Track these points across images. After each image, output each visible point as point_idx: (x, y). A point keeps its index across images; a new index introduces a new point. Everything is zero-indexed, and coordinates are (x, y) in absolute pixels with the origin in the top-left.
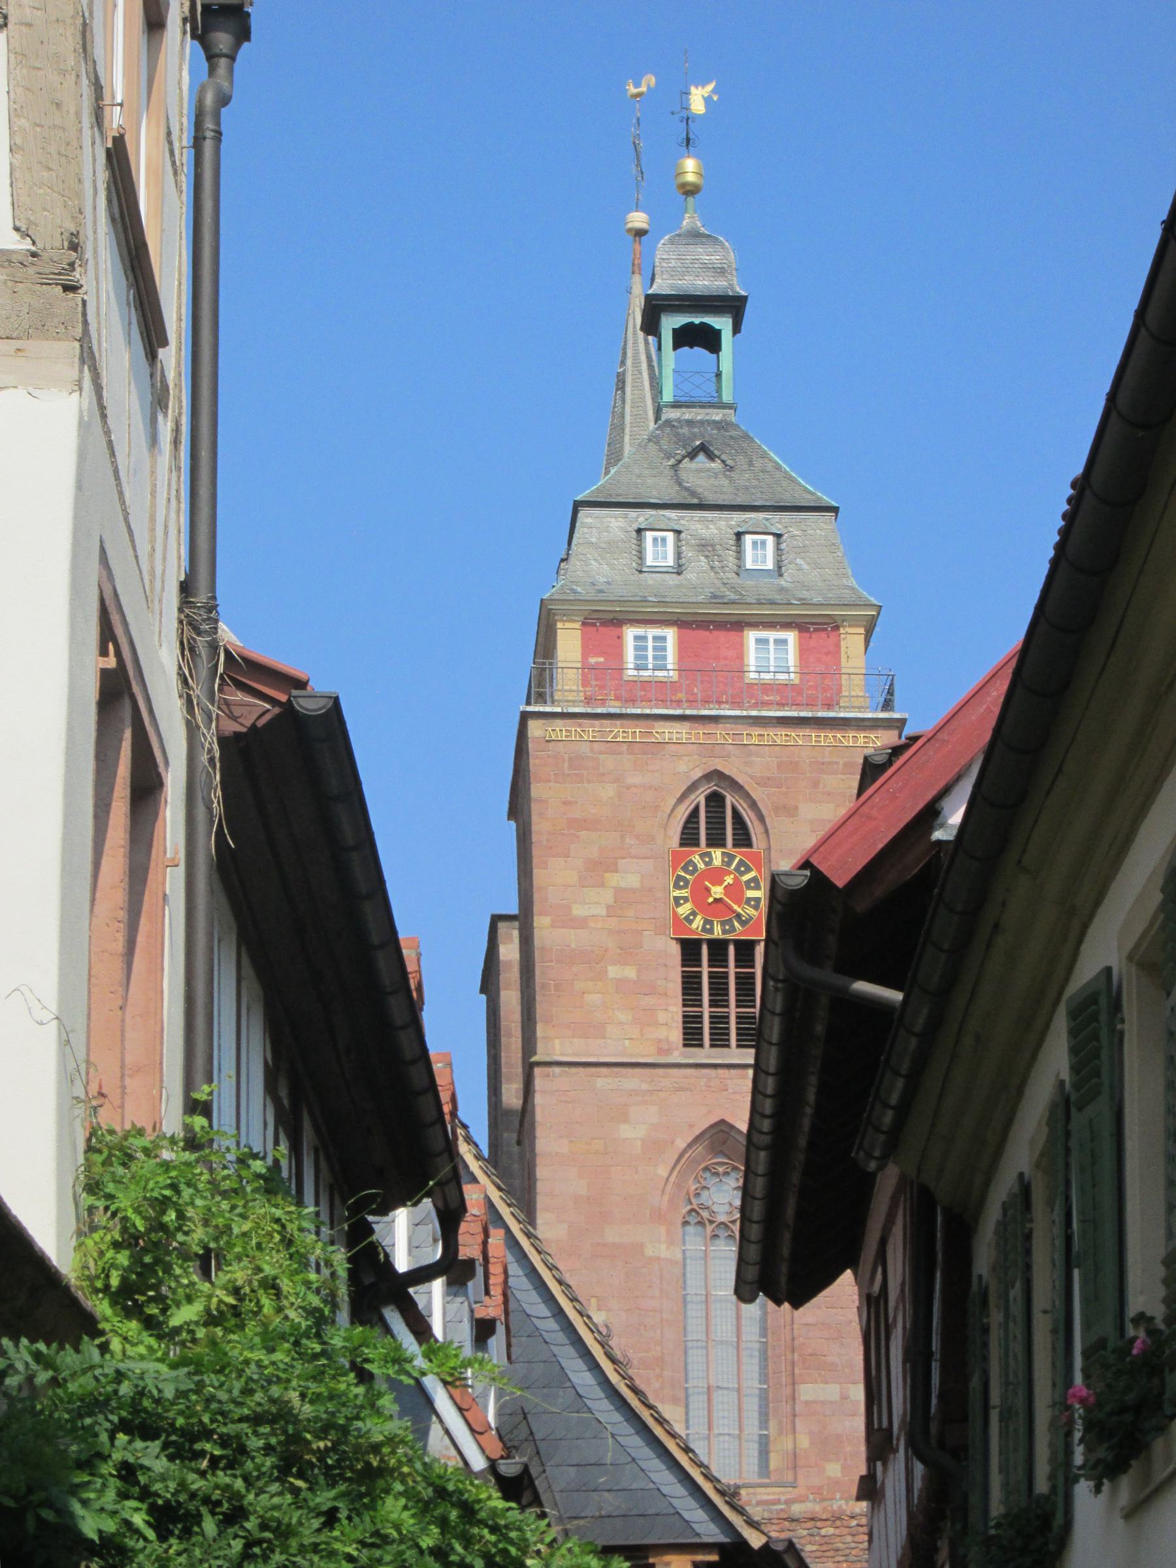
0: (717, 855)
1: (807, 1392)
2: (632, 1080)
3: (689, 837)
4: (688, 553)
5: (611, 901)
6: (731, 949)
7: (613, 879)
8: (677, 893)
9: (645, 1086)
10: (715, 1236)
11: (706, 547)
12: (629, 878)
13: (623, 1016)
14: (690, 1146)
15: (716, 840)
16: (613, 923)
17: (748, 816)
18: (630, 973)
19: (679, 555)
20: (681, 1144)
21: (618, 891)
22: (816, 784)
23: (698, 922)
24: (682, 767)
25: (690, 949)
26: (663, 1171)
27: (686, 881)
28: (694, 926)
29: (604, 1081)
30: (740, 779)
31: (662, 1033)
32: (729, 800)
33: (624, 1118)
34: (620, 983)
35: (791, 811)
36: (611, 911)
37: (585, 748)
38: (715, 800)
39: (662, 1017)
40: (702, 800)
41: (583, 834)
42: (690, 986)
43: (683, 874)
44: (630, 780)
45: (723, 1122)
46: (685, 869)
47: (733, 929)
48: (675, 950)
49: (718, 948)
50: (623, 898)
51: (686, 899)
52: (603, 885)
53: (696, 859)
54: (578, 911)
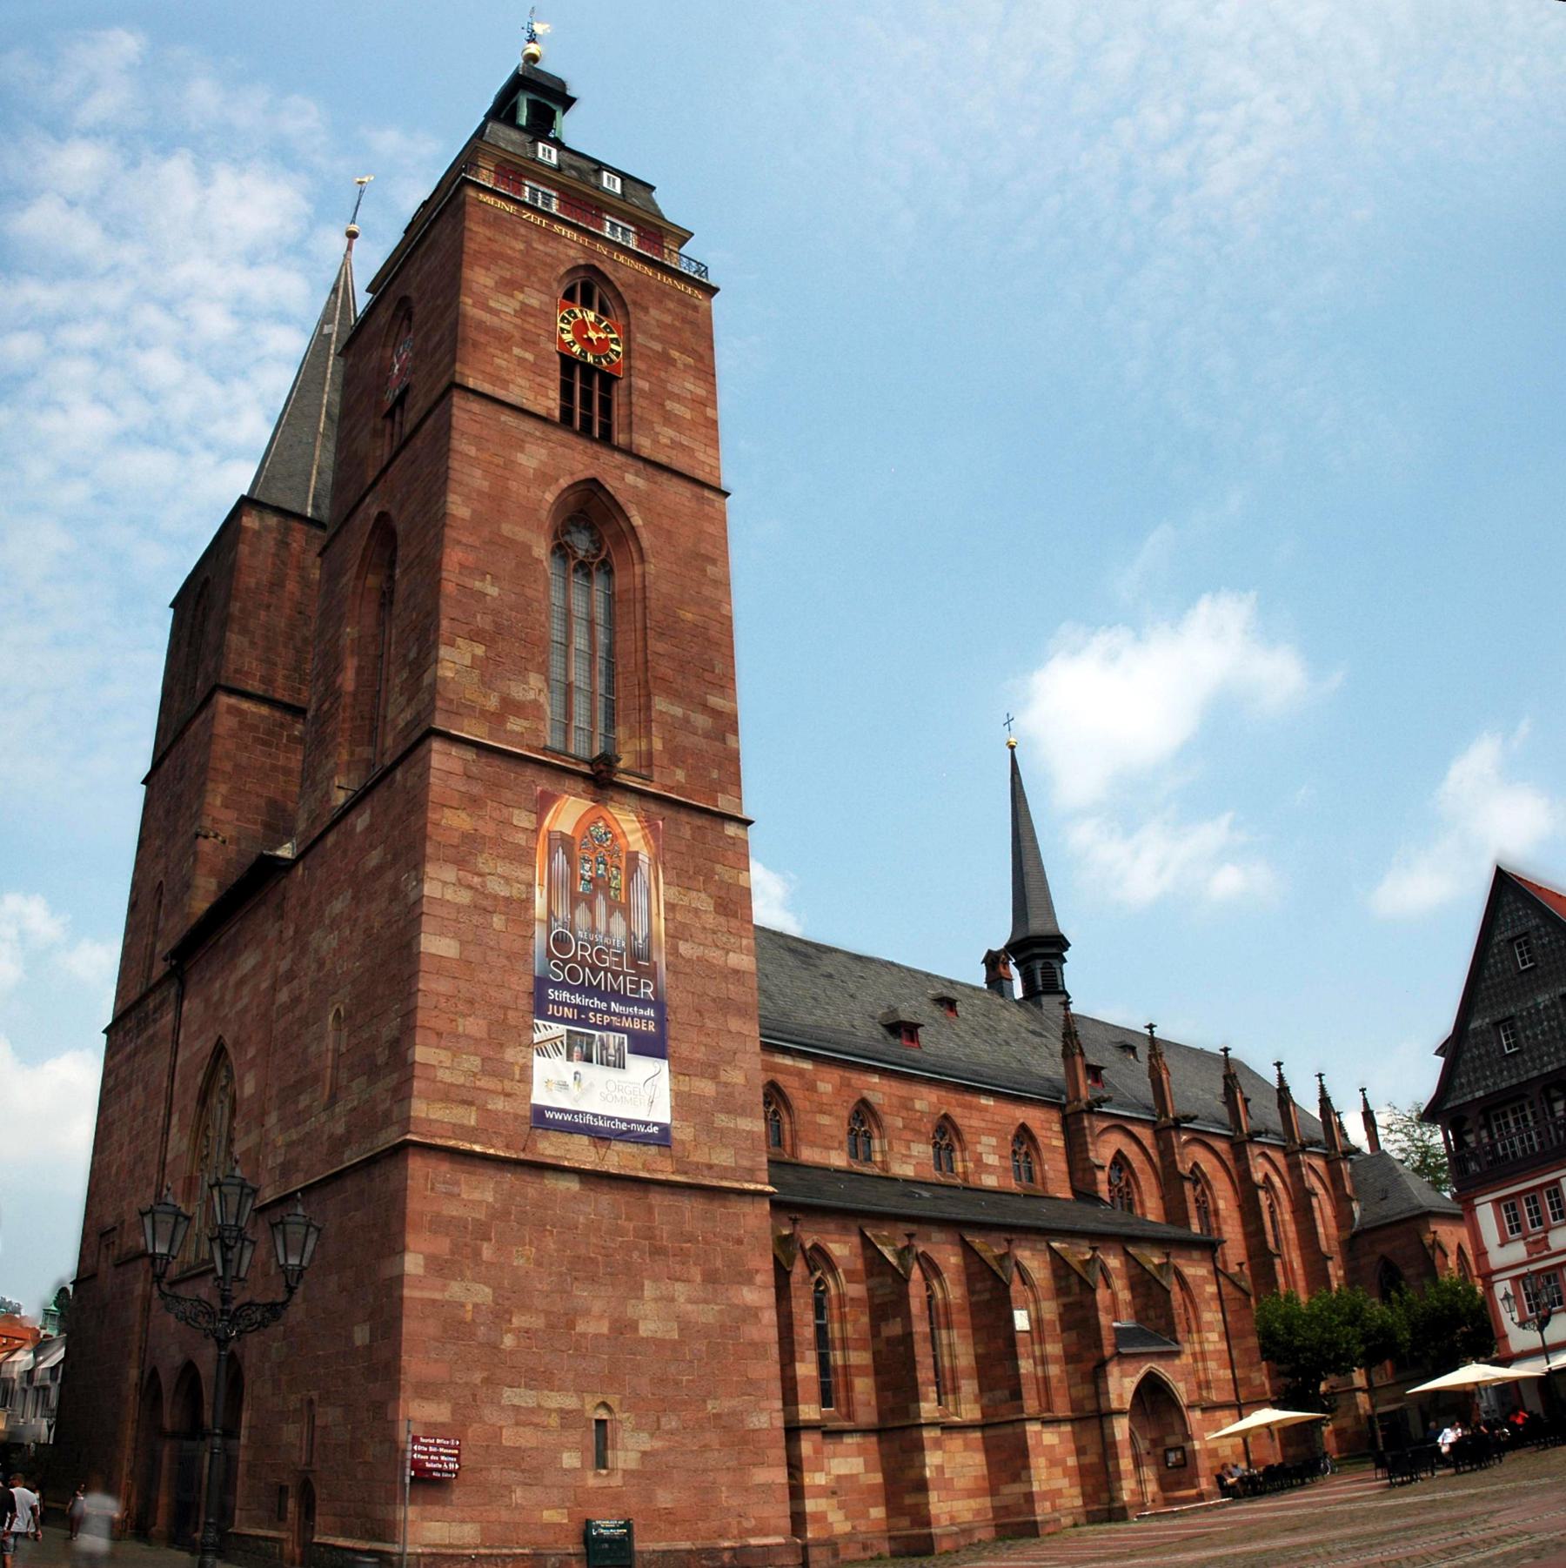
0: (591, 316)
5: (518, 308)
8: (563, 326)
9: (538, 434)
16: (519, 321)
18: (530, 357)
21: (523, 303)
23: (576, 349)
24: (572, 253)
25: (568, 363)
26: (550, 497)
28: (574, 349)
29: (507, 418)
33: (522, 450)
34: (521, 361)
35: (646, 310)
40: (579, 281)
41: (500, 262)
42: (566, 391)
44: (535, 245)
45: (594, 481)
46: (569, 313)
50: (525, 311)
51: (568, 332)
52: (512, 296)
53: (577, 311)
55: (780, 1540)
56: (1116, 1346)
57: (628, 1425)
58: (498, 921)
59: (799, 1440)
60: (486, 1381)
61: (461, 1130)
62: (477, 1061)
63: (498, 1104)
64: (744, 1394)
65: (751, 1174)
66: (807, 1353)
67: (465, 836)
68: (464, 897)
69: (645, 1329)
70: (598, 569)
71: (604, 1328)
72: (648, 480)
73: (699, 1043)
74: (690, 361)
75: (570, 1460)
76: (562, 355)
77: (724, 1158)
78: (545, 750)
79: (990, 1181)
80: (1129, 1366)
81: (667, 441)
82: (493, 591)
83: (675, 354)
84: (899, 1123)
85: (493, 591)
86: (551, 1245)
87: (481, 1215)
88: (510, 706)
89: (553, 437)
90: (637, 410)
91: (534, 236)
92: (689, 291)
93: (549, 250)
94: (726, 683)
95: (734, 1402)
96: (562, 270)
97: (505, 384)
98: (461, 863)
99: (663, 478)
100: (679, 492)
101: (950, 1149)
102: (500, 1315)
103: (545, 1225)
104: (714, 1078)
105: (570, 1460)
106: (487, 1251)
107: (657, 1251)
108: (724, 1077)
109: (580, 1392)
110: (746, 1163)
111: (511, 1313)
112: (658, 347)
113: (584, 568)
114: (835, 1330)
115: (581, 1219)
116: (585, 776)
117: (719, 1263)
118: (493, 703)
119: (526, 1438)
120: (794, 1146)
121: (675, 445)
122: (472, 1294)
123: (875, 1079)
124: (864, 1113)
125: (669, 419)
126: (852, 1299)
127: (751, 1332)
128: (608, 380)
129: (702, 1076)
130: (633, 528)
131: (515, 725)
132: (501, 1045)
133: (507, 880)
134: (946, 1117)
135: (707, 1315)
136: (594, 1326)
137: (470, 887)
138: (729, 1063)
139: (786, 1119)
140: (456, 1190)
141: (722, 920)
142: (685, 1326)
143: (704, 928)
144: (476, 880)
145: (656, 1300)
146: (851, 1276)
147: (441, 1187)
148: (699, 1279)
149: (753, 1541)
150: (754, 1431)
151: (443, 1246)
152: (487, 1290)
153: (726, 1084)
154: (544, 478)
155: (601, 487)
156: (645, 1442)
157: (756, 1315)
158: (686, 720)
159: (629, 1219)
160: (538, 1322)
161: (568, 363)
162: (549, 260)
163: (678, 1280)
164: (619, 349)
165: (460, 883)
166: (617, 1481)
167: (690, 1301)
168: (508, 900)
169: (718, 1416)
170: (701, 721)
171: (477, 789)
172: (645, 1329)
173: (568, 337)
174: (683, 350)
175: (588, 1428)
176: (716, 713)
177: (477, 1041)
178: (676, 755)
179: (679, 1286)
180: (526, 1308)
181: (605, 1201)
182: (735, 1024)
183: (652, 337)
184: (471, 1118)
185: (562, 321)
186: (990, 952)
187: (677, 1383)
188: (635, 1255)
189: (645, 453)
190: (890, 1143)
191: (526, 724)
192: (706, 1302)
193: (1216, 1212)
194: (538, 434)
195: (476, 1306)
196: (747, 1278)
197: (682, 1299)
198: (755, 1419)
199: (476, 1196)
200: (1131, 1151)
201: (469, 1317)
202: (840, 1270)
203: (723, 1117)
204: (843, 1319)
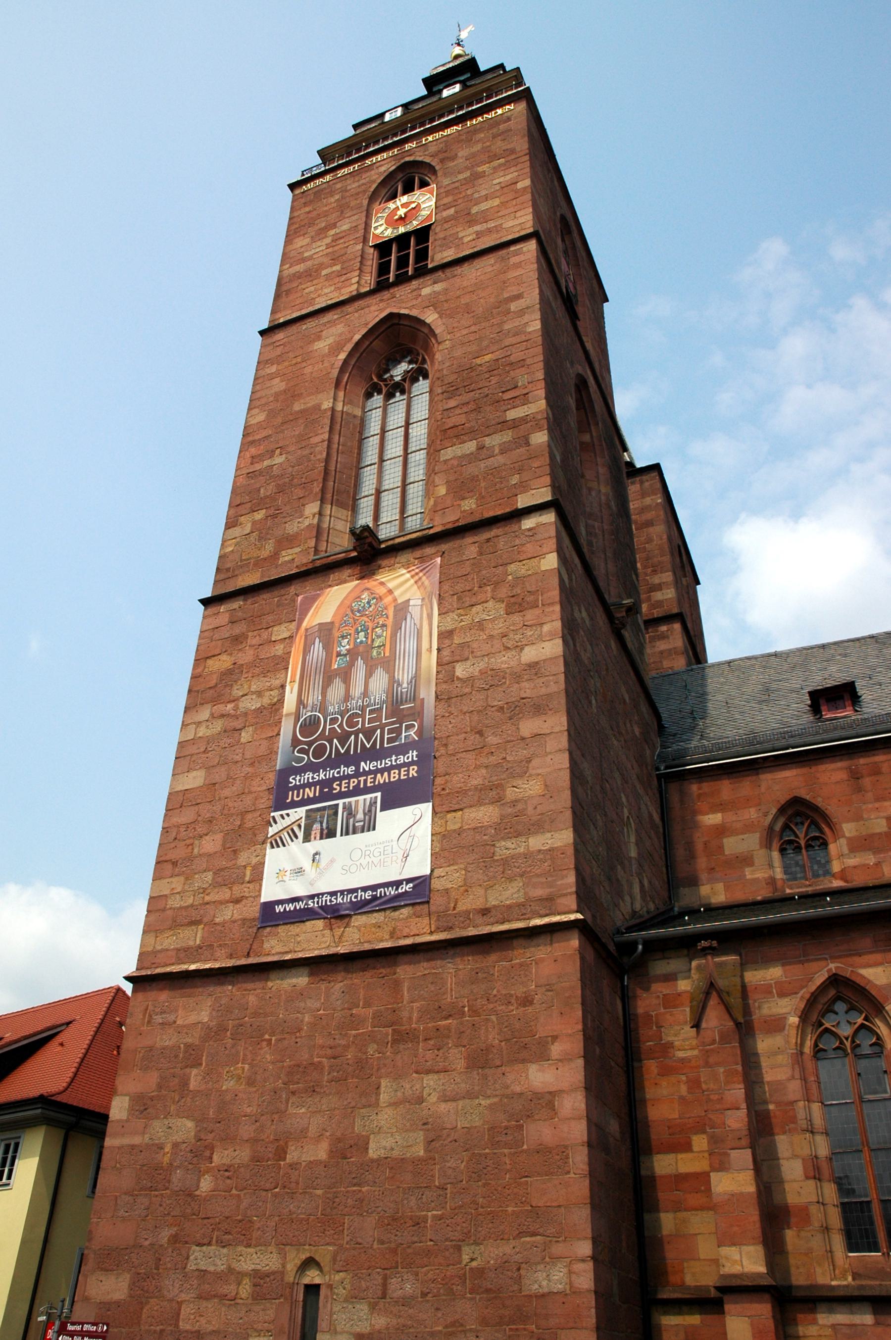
20: (357, 337)
24: (383, 169)
29: (305, 326)
34: (328, 277)
61: (188, 953)
62: (209, 876)
64: (520, 1234)
65: (549, 903)
66: (734, 1154)
71: (321, 1152)
73: (477, 767)
86: (267, 1055)
87: (193, 1039)
95: (506, 1249)
98: (215, 701)
103: (263, 1035)
104: (498, 800)
107: (402, 1037)
108: (510, 794)
109: (282, 1245)
110: (539, 892)
111: (212, 1149)
117: (493, 1037)
129: (480, 803)
132: (235, 852)
133: (259, 694)
138: (521, 776)
140: (172, 1018)
141: (516, 618)
143: (491, 637)
144: (230, 706)
145: (394, 1104)
147: (158, 1019)
152: (190, 1124)
153: (514, 803)
154: (335, 349)
155: (399, 315)
157: (551, 1106)
159: (367, 1005)
163: (428, 1072)
169: (480, 1272)
171: (238, 629)
177: (210, 855)
179: (430, 1080)
180: (228, 1139)
182: (528, 727)
184: (194, 936)
188: (372, 1049)
191: (297, 550)
192: (470, 1095)
195: (176, 1145)
196: (541, 1055)
197: (433, 1098)
198: (541, 1276)
199: (193, 1018)
201: (166, 1159)
203: (509, 844)
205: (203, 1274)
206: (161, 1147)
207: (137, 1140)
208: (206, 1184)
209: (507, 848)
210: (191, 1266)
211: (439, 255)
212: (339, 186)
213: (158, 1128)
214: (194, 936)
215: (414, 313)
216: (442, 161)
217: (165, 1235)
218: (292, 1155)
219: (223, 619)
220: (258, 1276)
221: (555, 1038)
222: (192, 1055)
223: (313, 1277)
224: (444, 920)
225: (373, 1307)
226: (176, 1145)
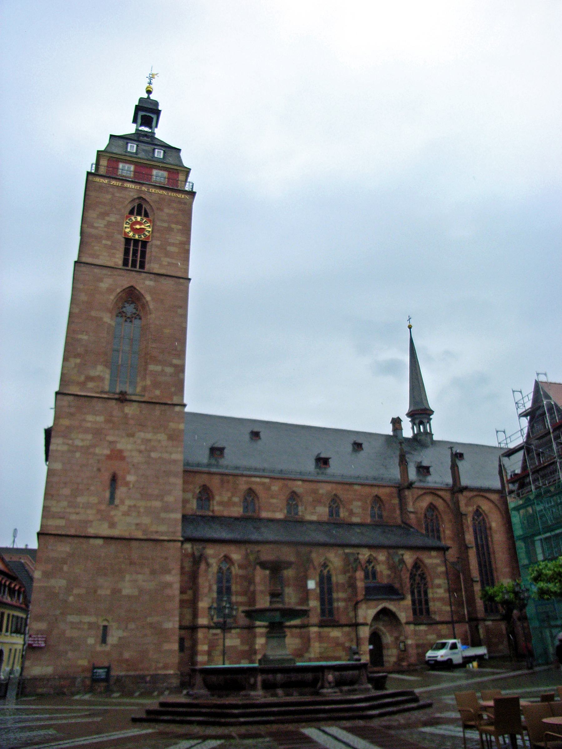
0: (139, 218)
1: (152, 367)
2: (105, 271)
3: (131, 212)
4: (139, 151)
6: (140, 244)
7: (107, 218)
9: (109, 273)
10: (126, 321)
11: (144, 151)
12: (113, 218)
13: (105, 254)
14: (121, 291)
15: (139, 214)
16: (106, 229)
17: (148, 211)
18: (109, 243)
19: (137, 150)
21: (109, 222)
22: (169, 205)
24: (132, 194)
26: (112, 297)
27: (129, 223)
29: (97, 270)
30: (148, 200)
31: (117, 260)
32: (144, 206)
34: (106, 245)
35: (162, 210)
36: (106, 226)
37: (104, 185)
38: (140, 206)
39: (117, 256)
40: (136, 205)
43: (128, 221)
45: (132, 287)
46: (129, 220)
47: (141, 237)
48: (123, 240)
49: (136, 242)
50: (109, 224)
51: (128, 228)
52: (104, 219)
54: (96, 225)
55: (171, 672)
56: (365, 595)
57: (114, 627)
58: (78, 455)
59: (197, 631)
60: (63, 614)
61: (57, 527)
63: (74, 517)
65: (174, 533)
67: (68, 427)
68: (65, 448)
69: (125, 592)
70: (135, 318)
71: (108, 592)
72: (155, 281)
74: (180, 227)
75: (91, 641)
76: (125, 238)
77: (163, 528)
78: (102, 392)
79: (356, 520)
80: (373, 603)
81: (166, 264)
82: (85, 337)
83: (173, 226)
84: (311, 499)
85: (85, 337)
88: (89, 379)
89: (116, 273)
90: (154, 254)
91: (116, 190)
92: (183, 196)
93: (121, 195)
94: (181, 354)
96: (127, 202)
97: (97, 257)
98: (65, 437)
99: (163, 280)
100: (168, 284)
101: (338, 507)
102: (69, 590)
104: (162, 500)
105: (91, 641)
106: (65, 568)
107: (132, 563)
111: (72, 588)
112: (165, 225)
113: (130, 319)
114: (234, 588)
115: (103, 555)
116: (116, 399)
118: (82, 378)
119: (75, 634)
120: (259, 512)
121: (169, 264)
122: (59, 583)
123: (300, 483)
124: (294, 496)
125: (168, 254)
126: (241, 576)
127: (168, 592)
128: (145, 244)
130: (147, 302)
131: (90, 385)
133: (83, 440)
134: (335, 495)
135: (151, 586)
136: (104, 592)
137: (68, 444)
139: (256, 502)
141: (170, 443)
142: (141, 591)
144: (70, 442)
145: (131, 581)
146: (240, 567)
148: (148, 572)
149: (160, 672)
150: (166, 629)
151: (49, 567)
154: (110, 290)
155: (135, 289)
156: (121, 633)
158: (163, 370)
160: (83, 591)
161: (128, 241)
162: (121, 200)
164: (150, 230)
165: (64, 443)
166: (107, 648)
167: (144, 581)
168: (82, 447)
169: (151, 624)
170: (169, 370)
171: (73, 410)
172: (125, 592)
173: (128, 230)
174: (177, 223)
175: (99, 628)
176: (175, 366)
178: (156, 385)
181: (113, 547)
182: (172, 480)
183: (164, 221)
184: (62, 522)
185: (126, 224)
186: (432, 412)
187: (136, 611)
189: (156, 271)
190: (306, 509)
193: (490, 528)
194: (109, 273)
196: (169, 572)
200: (440, 504)
202: (236, 565)
204: (236, 583)
205: (72, 623)
206: (55, 587)
207: (46, 584)
208: (71, 599)
209: (163, 515)
210: (68, 620)
211: (152, 266)
212: (111, 190)
213: (53, 582)
214: (62, 522)
215: (142, 292)
216: (158, 209)
217: (58, 612)
218: (99, 592)
219: (65, 403)
220: (90, 624)
221: (173, 569)
222: (64, 561)
223: (106, 623)
224: (144, 532)
225: (124, 631)
226: (60, 587)
